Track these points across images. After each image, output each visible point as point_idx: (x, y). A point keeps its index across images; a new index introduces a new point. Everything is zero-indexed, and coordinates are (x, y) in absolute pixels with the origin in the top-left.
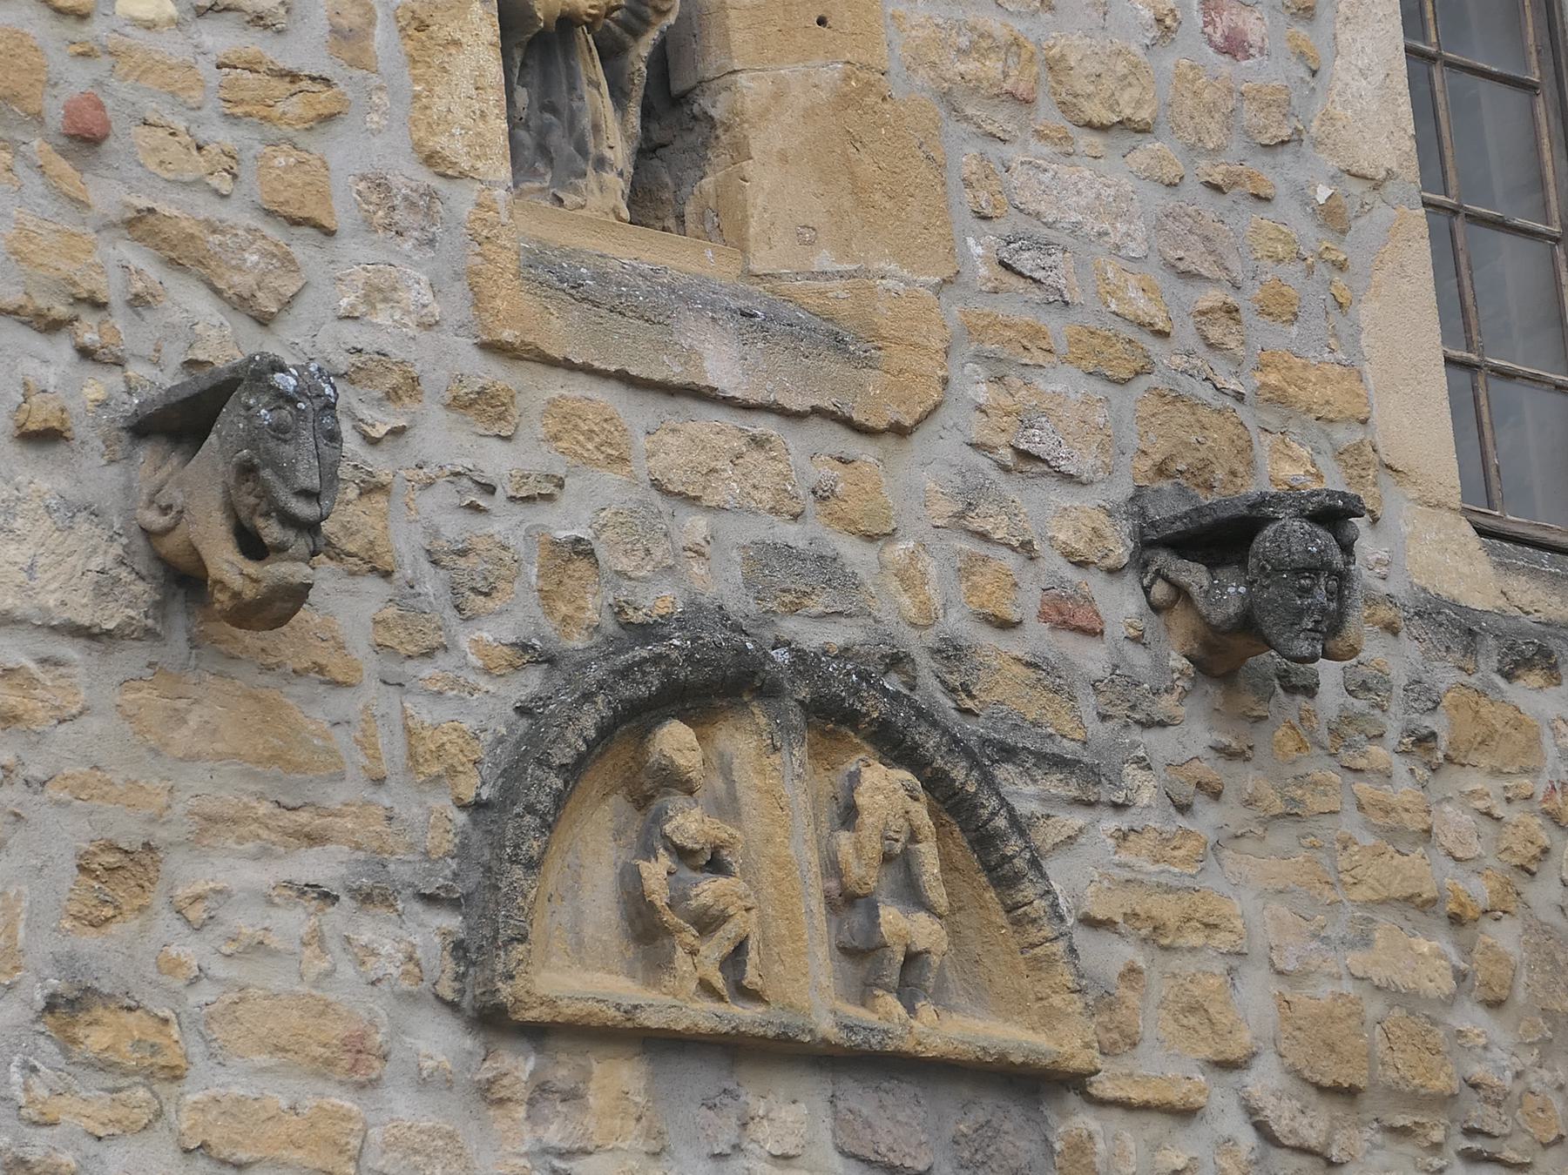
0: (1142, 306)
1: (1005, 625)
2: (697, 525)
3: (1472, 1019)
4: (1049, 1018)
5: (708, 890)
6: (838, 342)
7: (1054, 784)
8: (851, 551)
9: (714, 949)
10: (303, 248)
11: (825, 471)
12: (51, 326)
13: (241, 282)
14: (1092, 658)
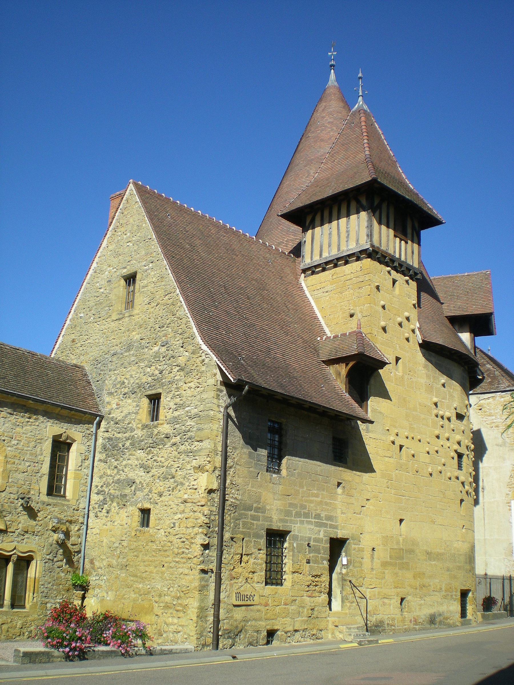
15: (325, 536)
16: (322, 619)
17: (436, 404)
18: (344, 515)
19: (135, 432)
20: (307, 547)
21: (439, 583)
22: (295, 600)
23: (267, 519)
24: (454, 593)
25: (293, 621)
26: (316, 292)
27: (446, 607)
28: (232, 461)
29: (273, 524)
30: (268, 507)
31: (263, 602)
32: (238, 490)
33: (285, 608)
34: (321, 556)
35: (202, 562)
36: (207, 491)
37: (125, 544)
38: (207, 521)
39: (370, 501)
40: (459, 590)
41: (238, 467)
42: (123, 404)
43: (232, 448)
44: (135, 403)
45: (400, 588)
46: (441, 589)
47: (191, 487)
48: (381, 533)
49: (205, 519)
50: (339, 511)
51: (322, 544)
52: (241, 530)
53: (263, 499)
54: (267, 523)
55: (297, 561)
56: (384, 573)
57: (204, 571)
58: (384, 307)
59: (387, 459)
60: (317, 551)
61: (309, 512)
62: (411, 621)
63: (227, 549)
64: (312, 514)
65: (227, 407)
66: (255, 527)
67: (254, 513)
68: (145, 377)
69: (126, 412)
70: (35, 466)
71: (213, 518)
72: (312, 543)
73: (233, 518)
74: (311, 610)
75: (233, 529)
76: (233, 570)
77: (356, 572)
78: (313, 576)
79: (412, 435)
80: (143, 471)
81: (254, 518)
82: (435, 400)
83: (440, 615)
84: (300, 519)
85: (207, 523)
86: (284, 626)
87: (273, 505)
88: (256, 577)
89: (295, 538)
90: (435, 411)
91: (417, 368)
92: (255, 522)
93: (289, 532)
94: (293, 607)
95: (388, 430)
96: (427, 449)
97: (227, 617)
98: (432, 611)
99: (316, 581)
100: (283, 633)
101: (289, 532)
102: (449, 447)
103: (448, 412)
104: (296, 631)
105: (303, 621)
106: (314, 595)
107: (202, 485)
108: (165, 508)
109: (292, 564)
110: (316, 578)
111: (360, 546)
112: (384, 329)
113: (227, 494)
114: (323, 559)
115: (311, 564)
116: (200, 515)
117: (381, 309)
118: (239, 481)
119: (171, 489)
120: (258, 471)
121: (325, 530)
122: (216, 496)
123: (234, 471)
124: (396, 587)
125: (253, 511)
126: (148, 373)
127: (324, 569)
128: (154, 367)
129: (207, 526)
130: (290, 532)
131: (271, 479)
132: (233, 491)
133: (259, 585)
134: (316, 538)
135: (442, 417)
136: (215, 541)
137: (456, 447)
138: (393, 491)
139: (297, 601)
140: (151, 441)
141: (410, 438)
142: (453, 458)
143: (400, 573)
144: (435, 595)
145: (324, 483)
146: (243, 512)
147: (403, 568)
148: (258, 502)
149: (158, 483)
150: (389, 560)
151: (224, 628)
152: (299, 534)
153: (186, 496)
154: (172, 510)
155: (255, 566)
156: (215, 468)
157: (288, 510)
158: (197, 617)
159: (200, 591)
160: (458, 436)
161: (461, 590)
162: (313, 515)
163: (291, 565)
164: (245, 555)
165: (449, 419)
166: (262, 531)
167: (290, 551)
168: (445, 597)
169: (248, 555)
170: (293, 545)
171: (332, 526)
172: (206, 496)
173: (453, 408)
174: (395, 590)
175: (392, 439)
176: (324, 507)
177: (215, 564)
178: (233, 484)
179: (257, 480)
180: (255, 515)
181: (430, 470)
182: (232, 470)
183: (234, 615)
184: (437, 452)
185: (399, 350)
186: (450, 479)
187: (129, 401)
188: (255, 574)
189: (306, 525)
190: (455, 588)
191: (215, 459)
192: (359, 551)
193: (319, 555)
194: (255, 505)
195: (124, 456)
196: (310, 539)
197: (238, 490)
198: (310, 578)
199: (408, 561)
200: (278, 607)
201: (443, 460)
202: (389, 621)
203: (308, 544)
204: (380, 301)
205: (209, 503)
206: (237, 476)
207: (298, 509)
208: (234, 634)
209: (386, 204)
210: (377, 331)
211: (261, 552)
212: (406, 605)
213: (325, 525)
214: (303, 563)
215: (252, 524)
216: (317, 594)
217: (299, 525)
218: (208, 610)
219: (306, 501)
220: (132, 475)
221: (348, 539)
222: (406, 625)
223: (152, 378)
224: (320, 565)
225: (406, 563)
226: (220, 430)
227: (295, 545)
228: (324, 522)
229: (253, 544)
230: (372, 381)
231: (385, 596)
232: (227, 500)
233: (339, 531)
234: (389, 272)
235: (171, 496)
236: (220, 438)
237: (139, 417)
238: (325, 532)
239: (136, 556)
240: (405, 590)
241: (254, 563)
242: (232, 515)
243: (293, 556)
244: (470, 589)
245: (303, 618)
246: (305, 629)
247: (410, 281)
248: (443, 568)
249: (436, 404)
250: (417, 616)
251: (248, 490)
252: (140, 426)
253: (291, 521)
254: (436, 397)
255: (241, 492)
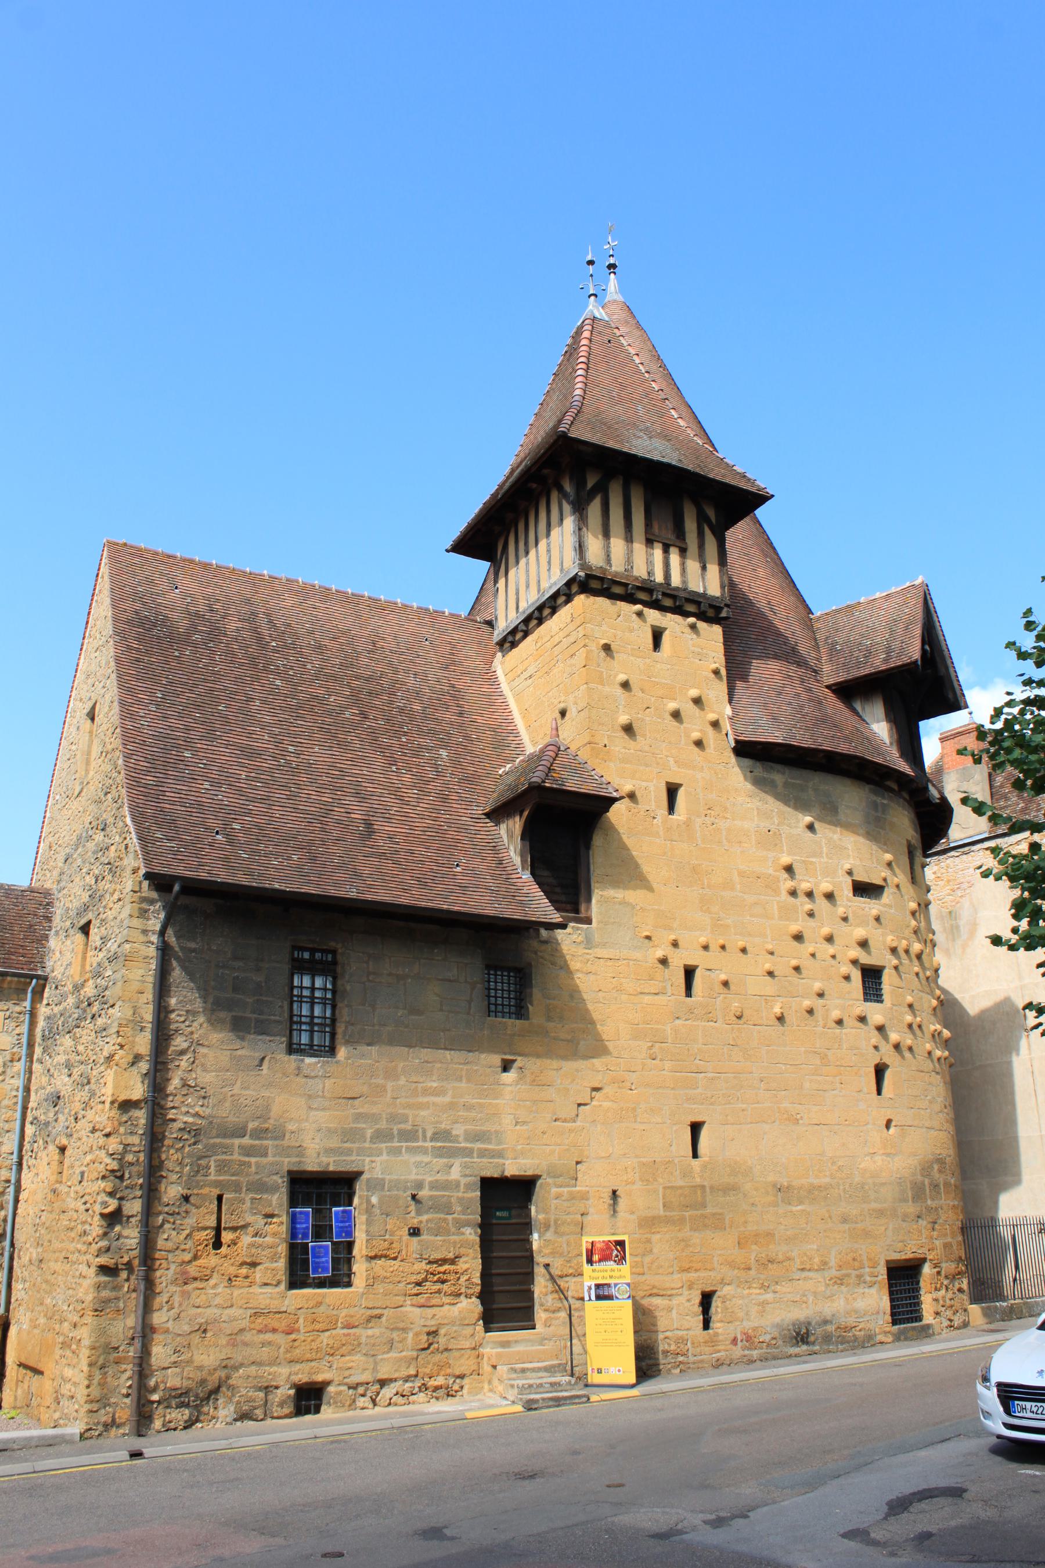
15: (466, 1176)
16: (463, 1351)
17: (789, 869)
18: (525, 1127)
20: (413, 1203)
21: (818, 1250)
22: (379, 1317)
23: (285, 1151)
24: (867, 1270)
25: (371, 1359)
27: (842, 1302)
28: (184, 1038)
29: (308, 1160)
30: (291, 1127)
31: (282, 1325)
32: (204, 1098)
33: (349, 1335)
34: (453, 1219)
35: (103, 1250)
36: (116, 1105)
38: (114, 1165)
39: (603, 1092)
40: (883, 1263)
41: (203, 1050)
43: (184, 1013)
45: (696, 1270)
46: (825, 1263)
48: (637, 1156)
49: (108, 1160)
50: (507, 1120)
51: (458, 1191)
52: (212, 1177)
53: (275, 1110)
54: (287, 1160)
55: (383, 1233)
56: (649, 1241)
57: (104, 1269)
58: (625, 685)
59: (647, 999)
60: (448, 1209)
61: (417, 1128)
62: (734, 1341)
63: (172, 1220)
64: (424, 1131)
65: (162, 933)
66: (253, 1169)
67: (251, 1142)
71: (130, 1158)
72: (424, 1193)
73: (190, 1155)
74: (428, 1334)
75: (190, 1177)
76: (190, 1262)
77: (565, 1246)
78: (430, 1262)
79: (721, 942)
81: (248, 1151)
82: (786, 860)
83: (826, 1322)
84: (389, 1144)
85: (113, 1171)
86: (347, 1373)
87: (307, 1120)
88: (258, 1274)
89: (376, 1185)
90: (790, 884)
91: (731, 799)
92: (253, 1160)
93: (359, 1174)
94: (370, 1332)
95: (648, 938)
96: (768, 966)
97: (175, 1362)
98: (799, 1314)
99: (439, 1273)
100: (345, 1388)
101: (359, 1174)
102: (834, 957)
103: (827, 882)
104: (383, 1383)
105: (401, 1359)
106: (434, 1302)
109: (367, 1241)
110: (441, 1265)
111: (578, 1188)
112: (629, 729)
113: (173, 1108)
114: (460, 1224)
115: (422, 1237)
116: (102, 1154)
117: (620, 691)
118: (206, 1078)
120: (258, 1055)
121: (466, 1162)
122: (141, 1116)
123: (192, 1059)
124: (687, 1270)
125: (247, 1137)
127: (464, 1244)
129: (116, 1177)
130: (359, 1174)
131: (299, 1068)
132: (190, 1100)
133: (268, 1290)
134: (437, 1181)
135: (810, 895)
136: (134, 1207)
137: (855, 953)
138: (668, 1065)
139: (384, 1319)
141: (714, 947)
142: (847, 978)
143: (696, 1238)
144: (805, 1279)
145: (460, 1064)
146: (218, 1140)
147: (705, 1226)
148: (264, 1117)
150: (662, 1213)
151: (168, 1385)
152: (388, 1177)
155: (253, 1250)
156: (137, 1058)
157: (352, 1128)
158: (90, 1365)
159: (96, 1310)
160: (860, 929)
161: (888, 1262)
162: (429, 1134)
163: (364, 1242)
164: (225, 1229)
165: (830, 896)
166: (275, 1177)
167: (362, 1214)
168: (840, 1281)
169: (234, 1229)
170: (368, 1201)
171: (482, 1153)
172: (117, 1116)
173: (841, 873)
174: (686, 1276)
175: (660, 954)
176: (460, 1113)
177: (136, 1253)
178: (189, 1086)
179: (260, 1072)
180: (252, 1146)
181: (777, 1010)
182: (185, 1058)
183: (195, 1357)
184: (797, 969)
185: (676, 769)
186: (840, 1022)
188: (259, 1268)
189: (405, 1157)
190: (870, 1259)
191: (137, 1039)
192: (573, 1198)
193: (450, 1217)
194: (251, 1126)
196: (420, 1185)
197: (204, 1098)
198: (423, 1266)
199: (720, 1211)
200: (327, 1334)
201: (817, 986)
202: (669, 1345)
203: (414, 1197)
204: (617, 675)
205: (122, 1130)
206: (199, 1070)
207: (383, 1125)
208: (197, 1396)
209: (621, 482)
210: (609, 737)
211: (275, 1220)
212: (717, 1307)
213: (469, 1153)
214: (401, 1236)
215: (242, 1164)
216: (446, 1300)
217: (385, 1157)
218: (121, 1349)
219: (409, 1106)
221: (538, 1177)
222: (719, 1351)
224: (453, 1238)
225: (714, 1214)
226: (151, 979)
227: (374, 1200)
228: (462, 1145)
229: (248, 1204)
230: (597, 841)
231: (655, 1291)
232: (174, 1120)
233: (507, 1162)
234: (640, 614)
236: (149, 995)
238: (465, 1166)
240: (710, 1273)
241: (252, 1245)
242: (187, 1149)
243: (369, 1223)
244: (922, 1256)
245: (404, 1354)
246: (409, 1376)
247: (702, 625)
248: (830, 1217)
249: (789, 869)
250: (755, 1329)
251: (232, 1096)
253: (361, 1152)
254: (789, 855)
255: (212, 1101)
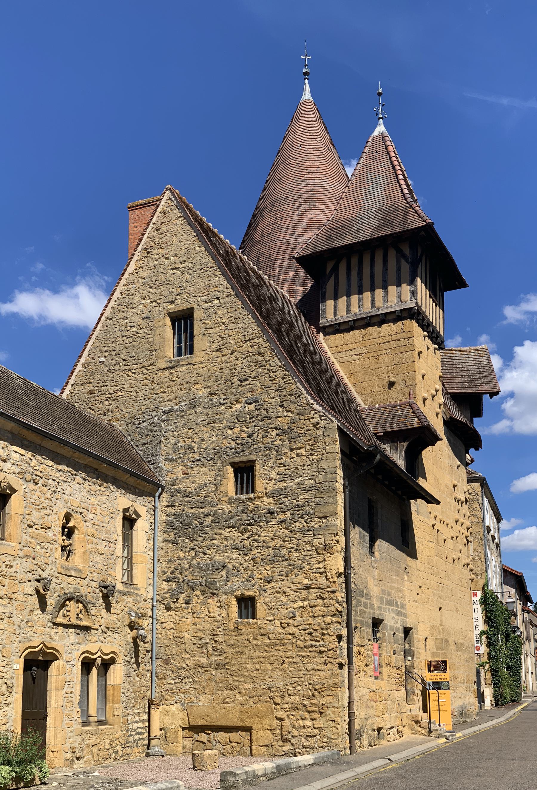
0: (101, 568)
1: (90, 593)
2: (70, 586)
3: (117, 622)
4: (90, 623)
5: (68, 613)
6: (81, 572)
7: (92, 605)
8: (80, 587)
9: (68, 618)
10: (47, 566)
11: (79, 581)
12: (31, 572)
13: (42, 568)
14: (95, 595)
19: (219, 507)
26: (341, 355)
37: (220, 639)
42: (193, 472)
44: (215, 472)
47: (315, 570)
68: (224, 441)
69: (198, 482)
70: (110, 547)
80: (238, 553)
107: (332, 568)
108: (278, 595)
119: (284, 573)
126: (230, 435)
128: (239, 429)
140: (245, 517)
149: (263, 566)
153: (306, 582)
154: (290, 597)
187: (204, 469)
195: (206, 536)
220: (218, 557)
223: (238, 442)
235: (285, 582)
237: (222, 489)
239: (239, 652)
252: (226, 499)
